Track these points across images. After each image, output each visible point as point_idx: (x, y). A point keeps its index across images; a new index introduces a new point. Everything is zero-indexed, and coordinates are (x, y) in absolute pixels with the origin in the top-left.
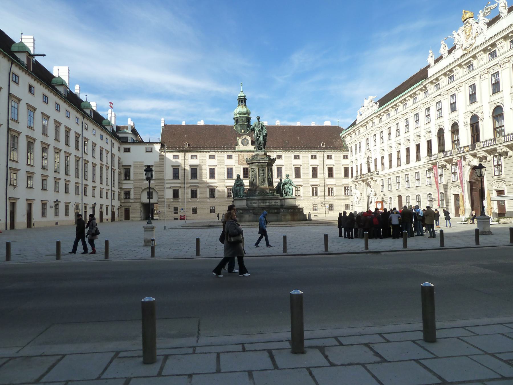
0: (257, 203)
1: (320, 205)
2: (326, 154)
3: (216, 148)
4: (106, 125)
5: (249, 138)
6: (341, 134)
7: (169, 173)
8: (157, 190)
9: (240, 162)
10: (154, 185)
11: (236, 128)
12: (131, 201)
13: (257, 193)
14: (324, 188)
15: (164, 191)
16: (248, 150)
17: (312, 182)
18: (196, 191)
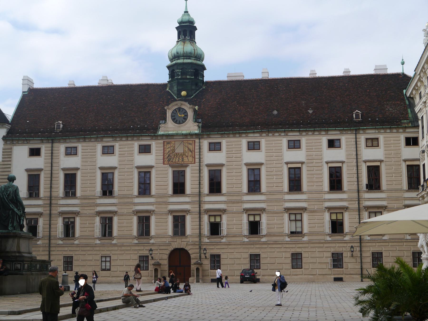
1: (349, 254)
2: (362, 138)
3: (117, 130)
5: (186, 107)
6: (404, 91)
14: (359, 215)
16: (184, 132)
17: (330, 200)
18: (73, 223)
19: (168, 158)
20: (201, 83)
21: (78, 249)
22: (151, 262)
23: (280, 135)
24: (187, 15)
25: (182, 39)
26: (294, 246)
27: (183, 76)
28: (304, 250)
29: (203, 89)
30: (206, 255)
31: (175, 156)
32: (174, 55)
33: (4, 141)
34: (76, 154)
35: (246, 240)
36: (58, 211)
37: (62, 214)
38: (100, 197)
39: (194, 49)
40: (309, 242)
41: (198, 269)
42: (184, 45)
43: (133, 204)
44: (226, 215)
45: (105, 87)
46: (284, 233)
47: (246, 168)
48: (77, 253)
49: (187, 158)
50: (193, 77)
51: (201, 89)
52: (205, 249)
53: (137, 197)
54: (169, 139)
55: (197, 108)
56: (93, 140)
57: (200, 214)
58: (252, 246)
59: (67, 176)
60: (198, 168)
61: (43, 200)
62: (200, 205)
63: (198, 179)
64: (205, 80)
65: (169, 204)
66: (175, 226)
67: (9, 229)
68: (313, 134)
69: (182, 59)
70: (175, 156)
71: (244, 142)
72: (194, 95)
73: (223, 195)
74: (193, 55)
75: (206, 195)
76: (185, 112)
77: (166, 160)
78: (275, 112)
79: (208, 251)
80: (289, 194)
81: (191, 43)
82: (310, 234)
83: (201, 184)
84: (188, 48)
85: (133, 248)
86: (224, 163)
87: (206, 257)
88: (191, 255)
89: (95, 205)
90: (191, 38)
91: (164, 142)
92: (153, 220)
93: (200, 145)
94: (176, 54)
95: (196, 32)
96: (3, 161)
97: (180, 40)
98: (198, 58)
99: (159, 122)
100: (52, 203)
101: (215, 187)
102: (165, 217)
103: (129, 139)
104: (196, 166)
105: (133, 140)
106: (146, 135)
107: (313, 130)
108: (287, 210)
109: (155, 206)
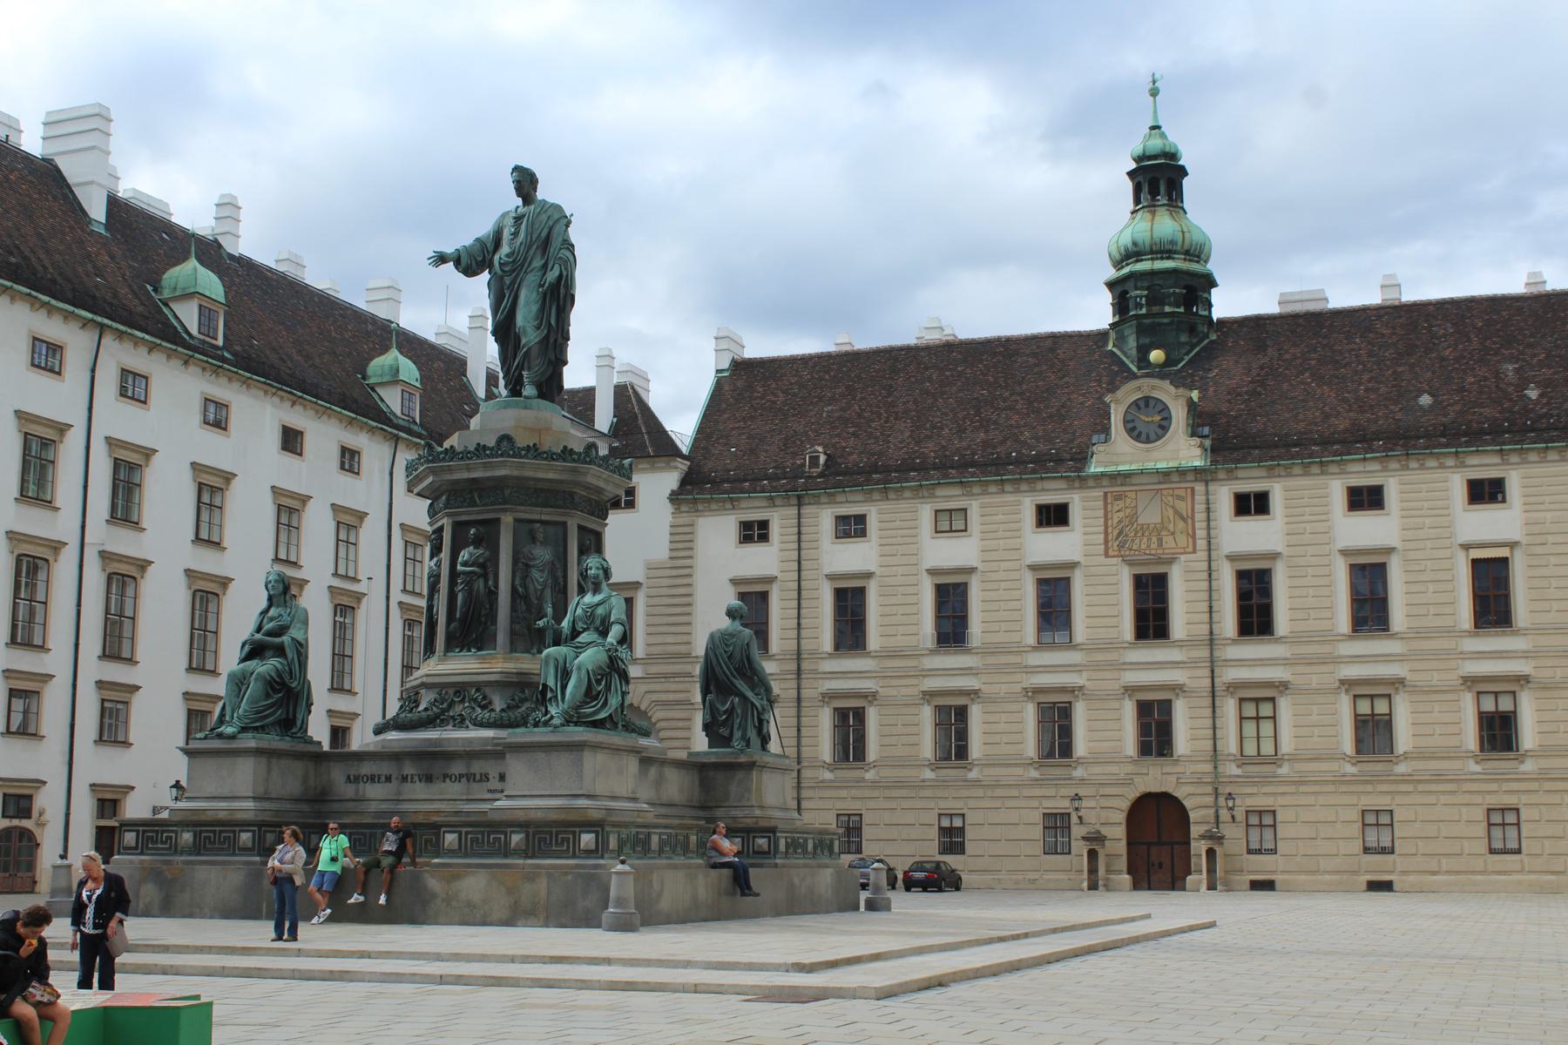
0: (388, 779)
3: (973, 464)
4: (382, 384)
5: (1165, 392)
8: (657, 714)
9: (1116, 541)
11: (1120, 341)
13: (421, 708)
19: (1120, 539)
20: (1206, 326)
21: (876, 793)
22: (1077, 831)
23: (1442, 466)
24: (1158, 136)
25: (1146, 204)
26: (1494, 787)
27: (1154, 308)
28: (1524, 799)
29: (1212, 342)
30: (1234, 813)
31: (1139, 534)
32: (1126, 250)
33: (672, 504)
34: (862, 533)
35: (1350, 769)
36: (820, 690)
37: (830, 697)
38: (932, 652)
39: (1183, 232)
40: (1542, 777)
41: (1211, 853)
42: (1153, 220)
43: (1025, 670)
44: (1289, 697)
45: (938, 346)
46: (1463, 749)
47: (1346, 565)
48: (872, 804)
49: (1171, 537)
50: (1182, 310)
51: (1206, 342)
52: (1230, 796)
53: (1035, 649)
54: (1118, 485)
55: (1195, 395)
56: (907, 494)
57: (1213, 697)
58: (1369, 788)
59: (840, 594)
60: (1204, 566)
61: (778, 662)
62: (1213, 671)
63: (1205, 596)
64: (1217, 314)
65: (1124, 667)
66: (1144, 729)
67: (735, 744)
68: (1543, 461)
69: (1149, 259)
70: (1139, 534)
71: (1336, 489)
72: (1187, 358)
73: (1280, 640)
74: (1179, 248)
75: (1229, 642)
76: (1163, 410)
77: (1112, 546)
78: (1425, 400)
79: (1238, 802)
80: (1476, 635)
81: (1174, 213)
82: (1544, 752)
83: (1214, 609)
84: (1164, 226)
85: (1026, 792)
86: (1279, 549)
87: (1233, 817)
88: (1190, 813)
89: (918, 673)
90: (1170, 199)
91: (1106, 493)
93: (1208, 500)
94: (1130, 245)
95: (1187, 183)
96: (671, 558)
97: (1140, 206)
98: (1195, 256)
99: (1090, 439)
100: (803, 668)
101: (1255, 619)
102: (1115, 705)
103: (1008, 488)
104: (1198, 560)
105: (1018, 491)
106: (1055, 477)
107: (1543, 448)
108: (1470, 681)
109: (1085, 675)
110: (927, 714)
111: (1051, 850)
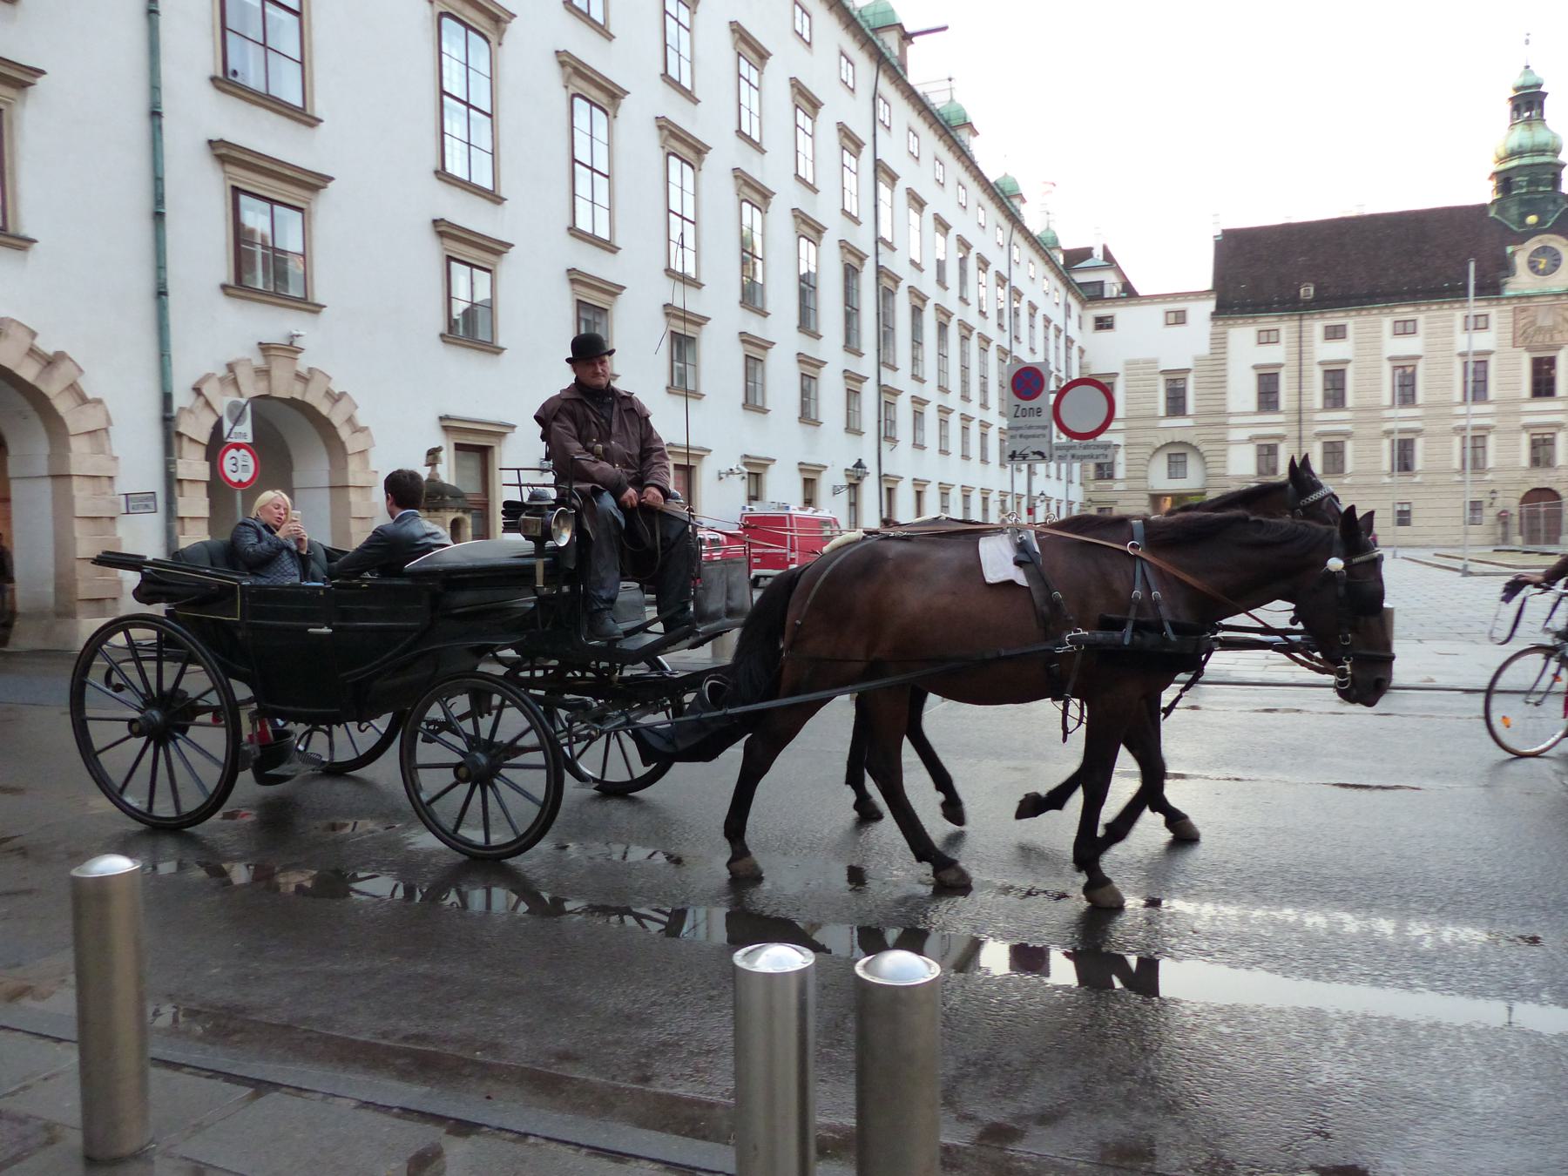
7: (1242, 393)
8: (1203, 448)
9: (1521, 337)
10: (1194, 432)
12: (1118, 486)
15: (1223, 453)
16: (1556, 290)
21: (1351, 492)
50: (1549, 189)
72: (1552, 220)
84: (1540, 136)
92: (1492, 440)
103: (1446, 306)
110: (1386, 443)
111: (1473, 522)
